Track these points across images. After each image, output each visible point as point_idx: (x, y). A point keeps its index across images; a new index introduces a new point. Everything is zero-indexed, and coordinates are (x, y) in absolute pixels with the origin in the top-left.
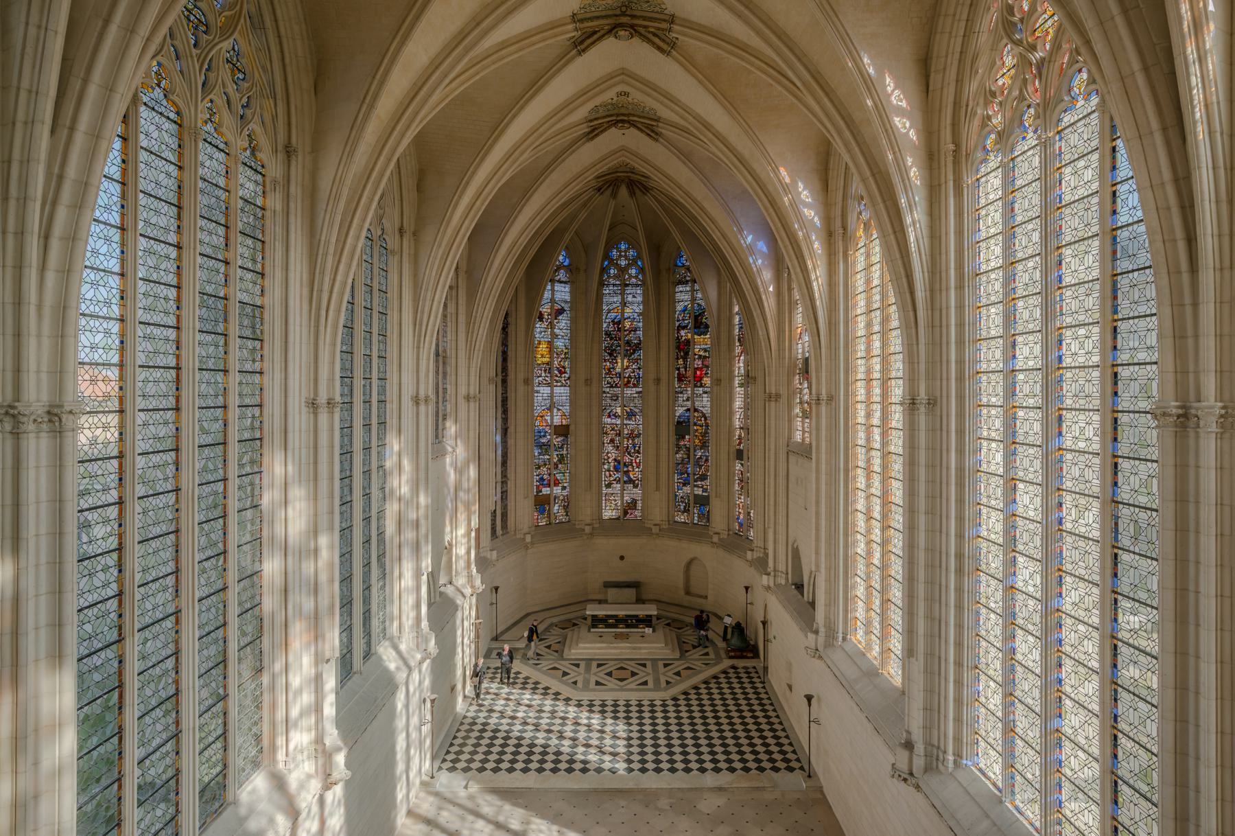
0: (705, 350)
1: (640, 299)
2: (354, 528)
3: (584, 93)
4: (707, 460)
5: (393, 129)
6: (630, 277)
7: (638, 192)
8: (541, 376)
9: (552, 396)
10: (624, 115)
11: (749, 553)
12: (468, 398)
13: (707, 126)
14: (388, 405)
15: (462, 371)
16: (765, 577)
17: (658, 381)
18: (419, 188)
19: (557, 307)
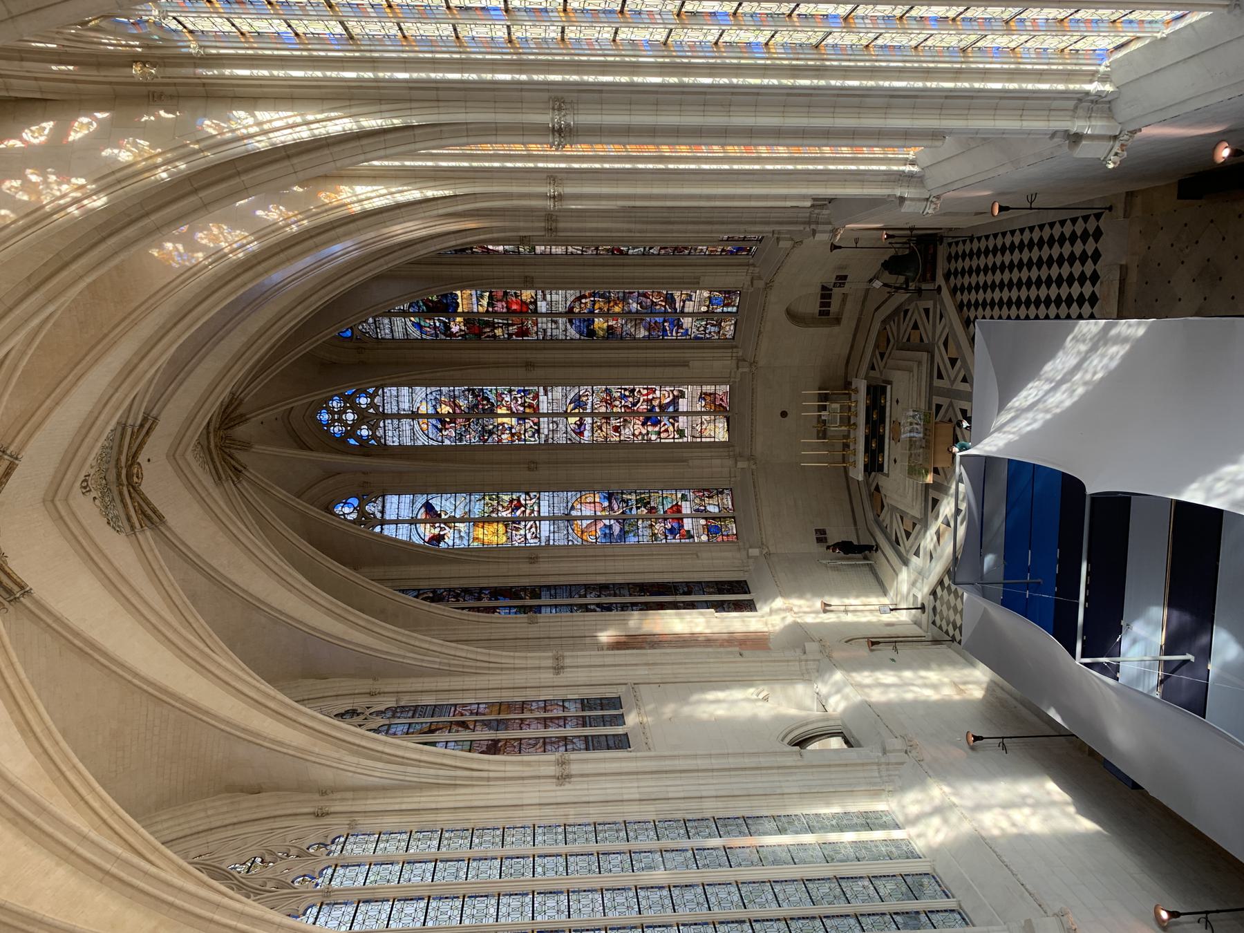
0: (482, 297)
1: (405, 390)
2: (740, 879)
3: (93, 559)
4: (645, 295)
5: (171, 905)
6: (372, 405)
7: (241, 410)
8: (523, 536)
9: (553, 519)
10: (119, 475)
11: (782, 244)
12: (558, 669)
13: (129, 370)
14: (571, 821)
15: (520, 678)
16: (819, 237)
17: (529, 365)
18: (256, 790)
19: (422, 515)
